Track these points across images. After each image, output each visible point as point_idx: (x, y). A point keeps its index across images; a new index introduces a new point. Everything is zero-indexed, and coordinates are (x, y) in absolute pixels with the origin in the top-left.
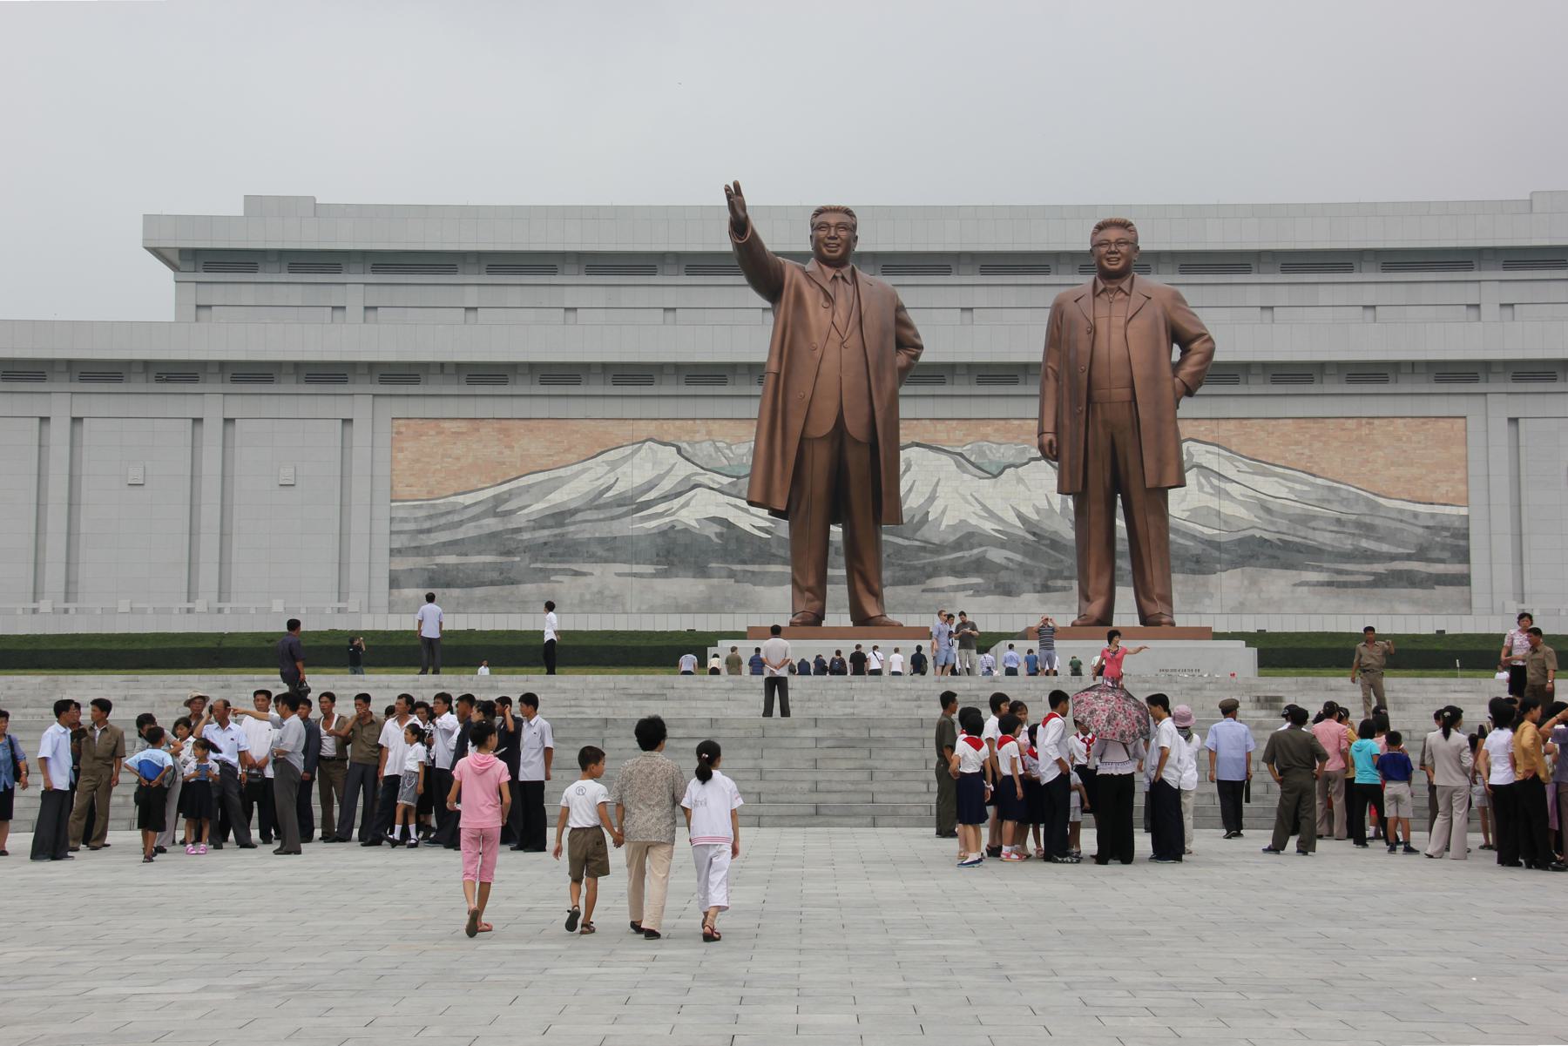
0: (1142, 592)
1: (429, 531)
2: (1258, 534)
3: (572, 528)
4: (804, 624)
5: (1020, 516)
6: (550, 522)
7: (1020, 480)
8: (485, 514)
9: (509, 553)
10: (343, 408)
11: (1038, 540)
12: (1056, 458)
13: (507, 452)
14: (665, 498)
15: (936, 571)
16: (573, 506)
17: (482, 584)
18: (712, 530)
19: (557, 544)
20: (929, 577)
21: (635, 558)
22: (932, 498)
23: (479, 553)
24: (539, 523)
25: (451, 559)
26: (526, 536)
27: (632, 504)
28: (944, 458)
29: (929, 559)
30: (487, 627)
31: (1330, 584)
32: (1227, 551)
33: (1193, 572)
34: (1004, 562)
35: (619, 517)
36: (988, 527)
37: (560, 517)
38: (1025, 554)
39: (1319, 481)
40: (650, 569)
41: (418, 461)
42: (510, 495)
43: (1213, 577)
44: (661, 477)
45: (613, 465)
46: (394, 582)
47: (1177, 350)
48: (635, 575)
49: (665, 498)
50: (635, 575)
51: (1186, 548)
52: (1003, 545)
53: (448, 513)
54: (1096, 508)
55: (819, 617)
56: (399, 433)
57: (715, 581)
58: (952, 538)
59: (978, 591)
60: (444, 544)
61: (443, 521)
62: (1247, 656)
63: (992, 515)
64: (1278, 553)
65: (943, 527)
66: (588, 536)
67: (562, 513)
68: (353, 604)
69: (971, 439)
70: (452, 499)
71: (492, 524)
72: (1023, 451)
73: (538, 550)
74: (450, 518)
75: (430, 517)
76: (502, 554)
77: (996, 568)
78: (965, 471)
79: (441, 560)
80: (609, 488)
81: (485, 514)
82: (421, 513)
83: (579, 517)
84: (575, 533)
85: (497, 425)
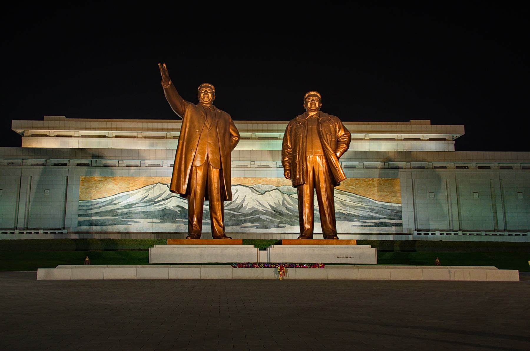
2: (341, 211)
5: (270, 206)
6: (128, 207)
7: (270, 195)
9: (115, 216)
11: (277, 213)
13: (115, 186)
14: (163, 200)
15: (245, 221)
16: (135, 202)
18: (177, 209)
19: (130, 213)
22: (244, 200)
24: (125, 207)
25: (98, 218)
26: (120, 211)
27: (153, 201)
28: (248, 188)
31: (362, 226)
34: (265, 219)
35: (149, 205)
36: (261, 209)
37: (131, 206)
38: (272, 217)
39: (358, 196)
40: (159, 221)
42: (116, 198)
44: (162, 194)
45: (148, 190)
48: (154, 222)
49: (163, 200)
50: (154, 222)
52: (265, 214)
57: (178, 224)
58: (250, 212)
59: (257, 227)
63: (262, 205)
64: (347, 217)
66: (139, 211)
69: (255, 183)
71: (110, 207)
72: (271, 187)
76: (113, 216)
77: (264, 220)
78: (254, 192)
79: (94, 218)
80: (146, 197)
83: (137, 205)
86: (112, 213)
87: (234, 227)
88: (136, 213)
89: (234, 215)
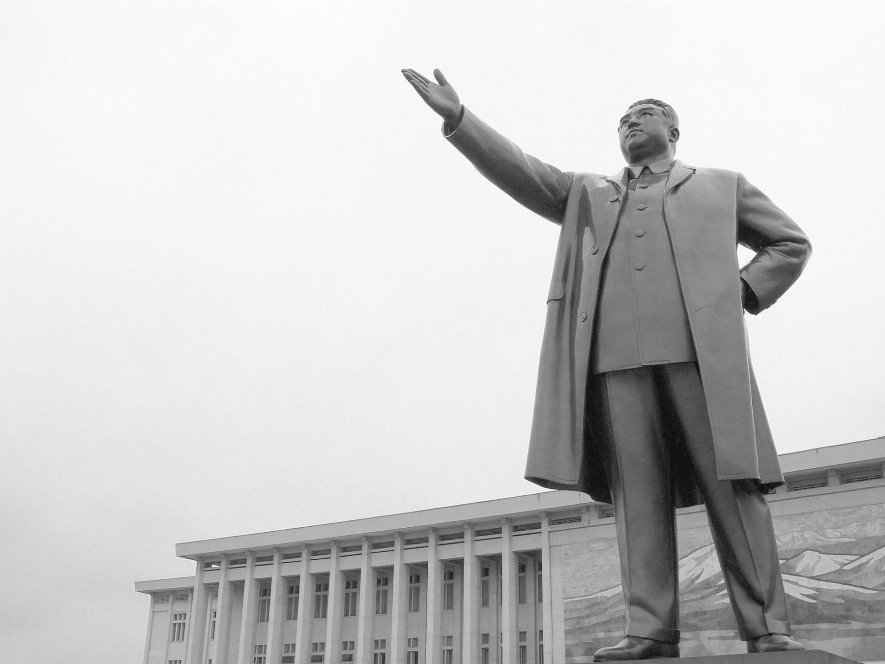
1: (587, 616)
25: (601, 635)
45: (699, 561)
70: (600, 594)
75: (587, 607)
80: (698, 577)
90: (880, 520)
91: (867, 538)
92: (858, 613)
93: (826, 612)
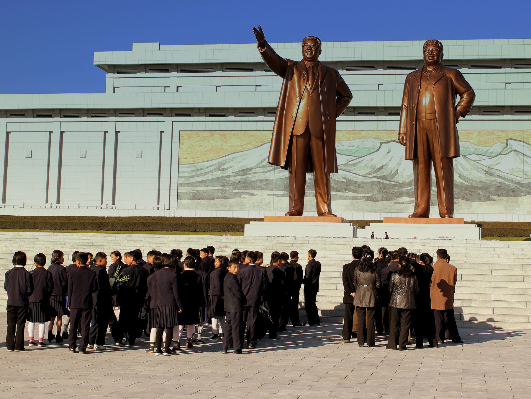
0: (440, 203)
1: (193, 176)
3: (250, 176)
4: (291, 214)
6: (241, 173)
8: (215, 170)
9: (224, 186)
10: (161, 126)
12: (405, 144)
13: (224, 144)
15: (400, 195)
16: (250, 166)
17: (213, 199)
19: (244, 182)
20: (398, 197)
21: (275, 188)
23: (213, 186)
24: (237, 174)
25: (201, 188)
26: (231, 179)
29: (397, 189)
30: (203, 216)
32: (526, 187)
33: (511, 196)
37: (245, 171)
40: (281, 193)
41: (190, 148)
43: (520, 199)
46: (178, 197)
47: (458, 97)
48: (275, 195)
50: (275, 195)
51: (509, 186)
53: (201, 169)
54: (421, 166)
55: (300, 213)
56: (182, 137)
58: (408, 181)
60: (199, 182)
61: (199, 172)
62: (477, 231)
65: (404, 176)
67: (246, 169)
68: (161, 206)
71: (219, 174)
73: (235, 185)
74: (201, 172)
75: (194, 171)
81: (215, 170)
82: (192, 169)
83: (253, 171)
84: (251, 178)
85: (221, 133)
86: (222, 181)
87: (385, 202)
88: (251, 182)
89: (385, 186)
90: (373, 139)
91: (364, 148)
92: (352, 187)
93: (335, 186)
